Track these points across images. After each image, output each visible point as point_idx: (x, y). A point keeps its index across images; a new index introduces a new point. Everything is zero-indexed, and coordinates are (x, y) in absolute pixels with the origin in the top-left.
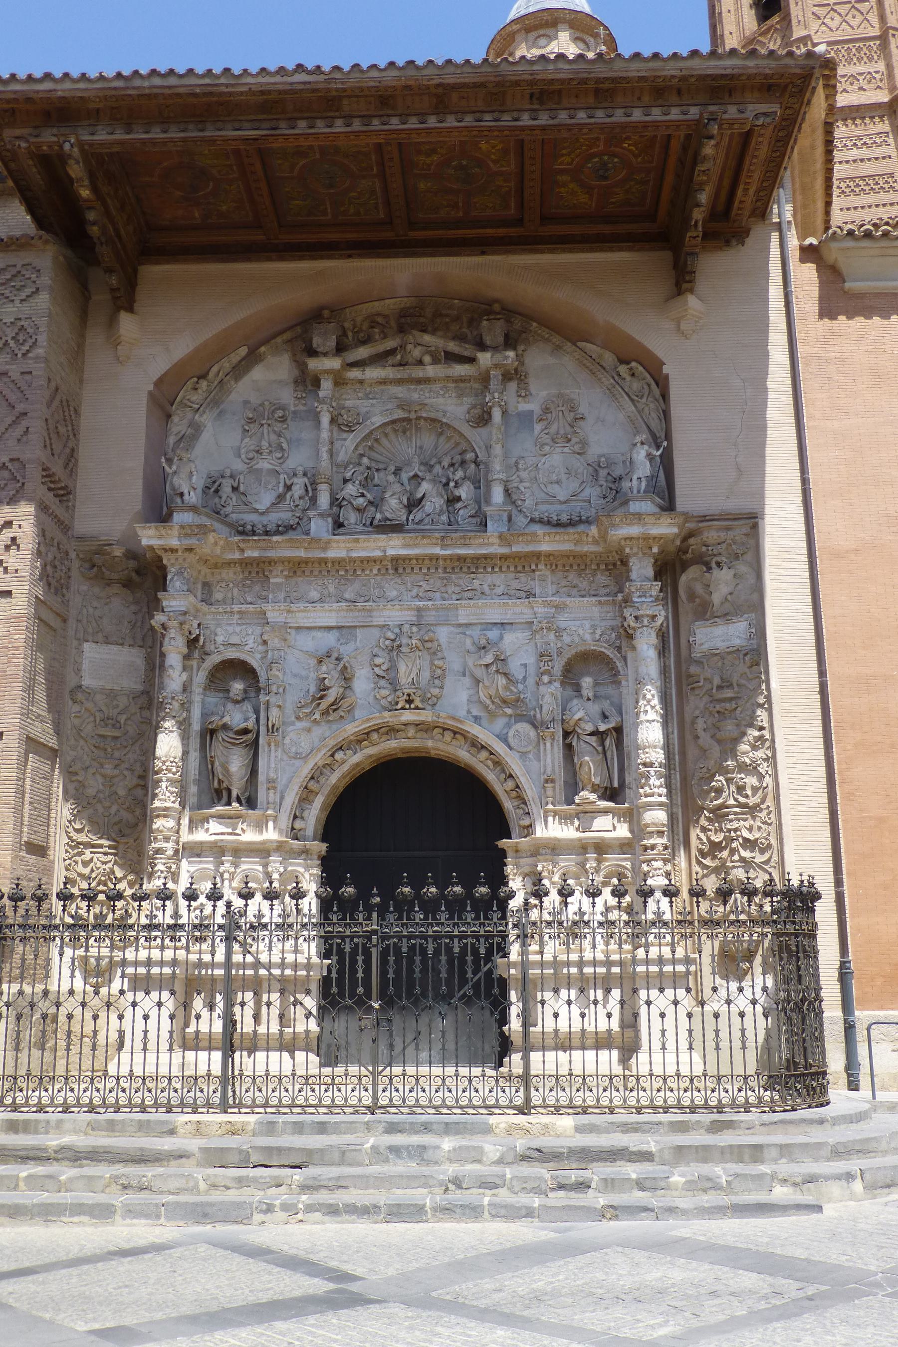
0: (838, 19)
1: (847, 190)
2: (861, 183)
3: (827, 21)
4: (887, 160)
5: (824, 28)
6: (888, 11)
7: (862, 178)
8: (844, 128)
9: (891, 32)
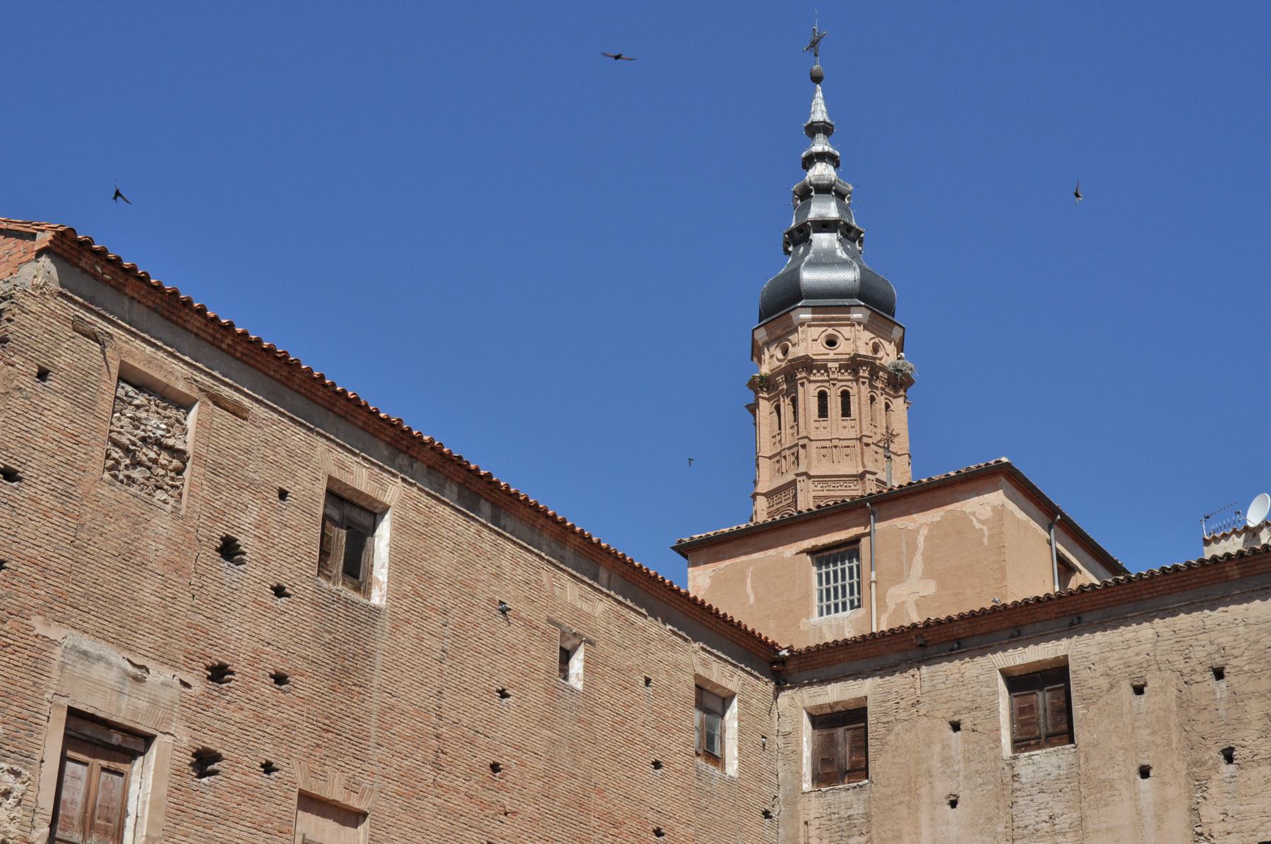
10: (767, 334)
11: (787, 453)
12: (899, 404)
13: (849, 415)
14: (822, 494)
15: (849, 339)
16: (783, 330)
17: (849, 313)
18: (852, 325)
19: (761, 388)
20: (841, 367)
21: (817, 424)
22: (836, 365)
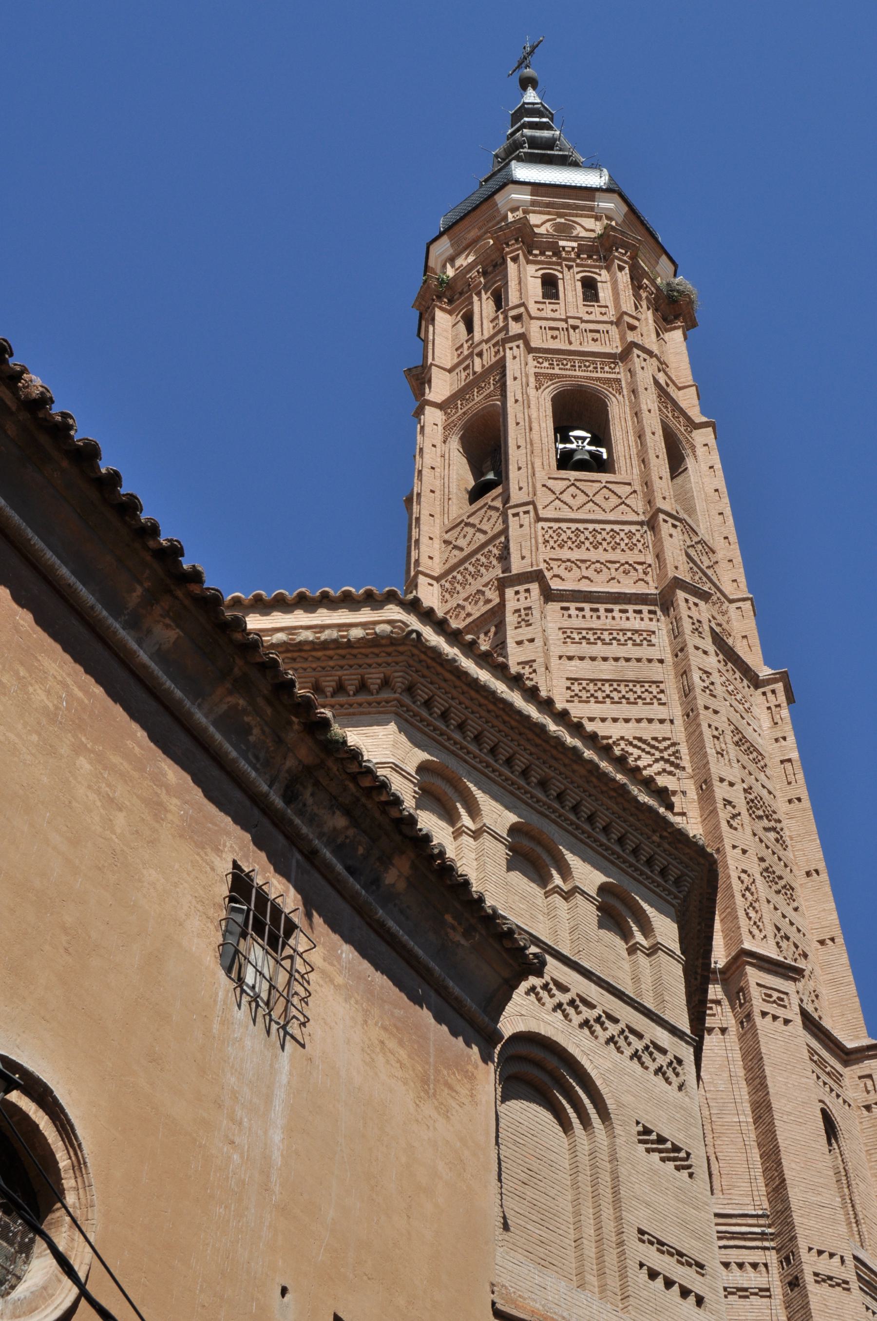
9: (662, 516)
10: (452, 245)
11: (485, 347)
12: (676, 337)
13: (596, 298)
14: (550, 371)
16: (480, 229)
17: (594, 201)
19: (439, 298)
20: (580, 250)
22: (575, 244)
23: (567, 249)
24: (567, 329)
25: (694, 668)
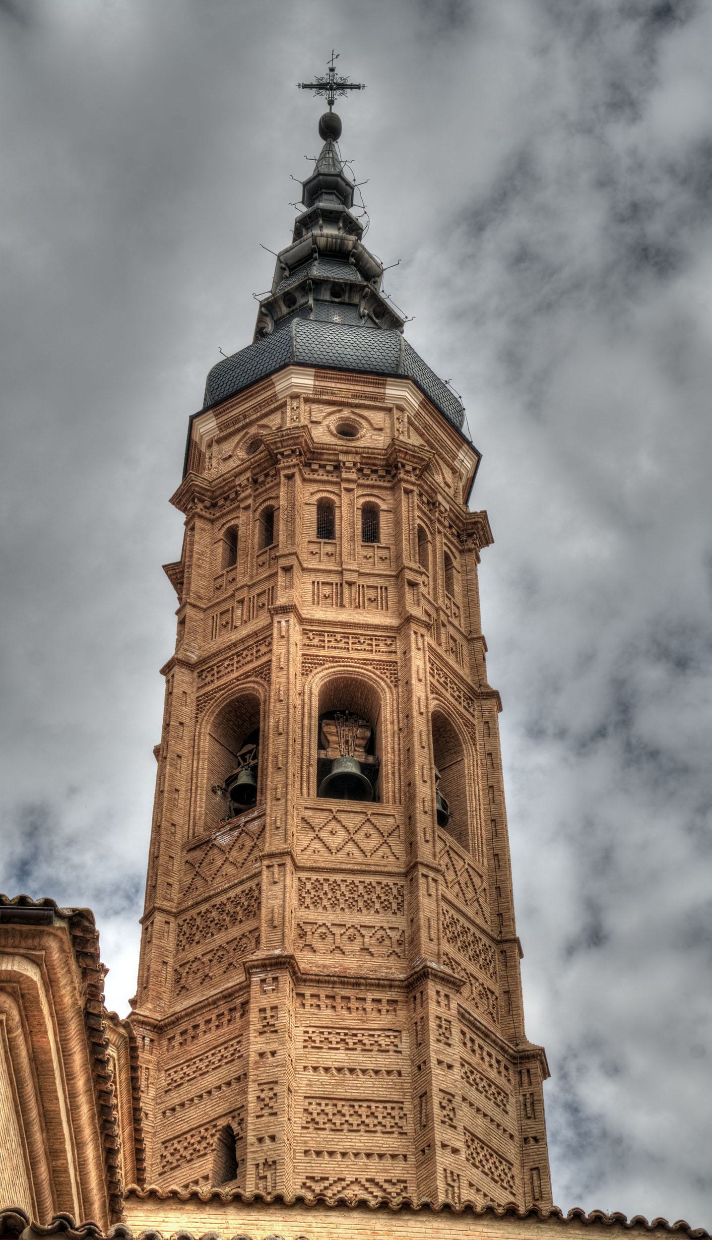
0: (342, 835)
1: (321, 1119)
2: (345, 1110)
3: (324, 835)
4: (394, 1077)
5: (317, 845)
6: (420, 837)
7: (351, 1101)
8: (329, 1012)
15: (381, 430)
18: (389, 410)
21: (314, 548)
23: (347, 464)
24: (341, 585)
25: (435, 1090)
